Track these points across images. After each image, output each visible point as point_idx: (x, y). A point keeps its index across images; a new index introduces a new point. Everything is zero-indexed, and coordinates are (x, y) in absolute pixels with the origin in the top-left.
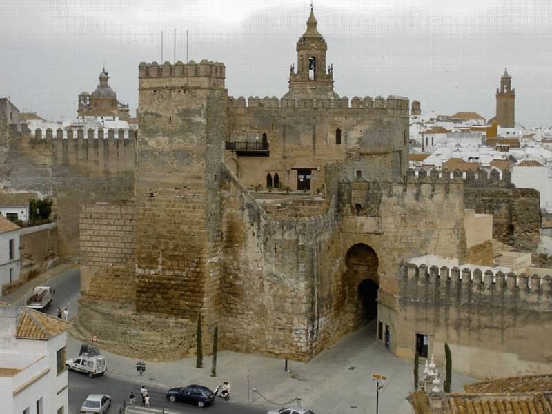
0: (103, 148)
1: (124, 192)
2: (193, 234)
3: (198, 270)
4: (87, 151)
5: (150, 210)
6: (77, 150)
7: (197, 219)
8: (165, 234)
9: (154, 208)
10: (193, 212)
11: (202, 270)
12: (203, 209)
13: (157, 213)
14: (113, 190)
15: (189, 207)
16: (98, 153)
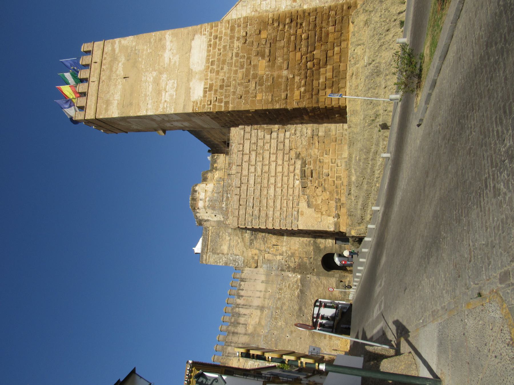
0: (240, 309)
1: (283, 295)
2: (244, 34)
3: (288, 21)
4: (239, 324)
5: (216, 91)
6: (237, 333)
7: (229, 31)
8: (244, 70)
9: (214, 88)
10: (221, 38)
11: (287, 15)
12: (217, 26)
13: (219, 83)
14: (279, 304)
15: (215, 43)
16: (245, 315)
